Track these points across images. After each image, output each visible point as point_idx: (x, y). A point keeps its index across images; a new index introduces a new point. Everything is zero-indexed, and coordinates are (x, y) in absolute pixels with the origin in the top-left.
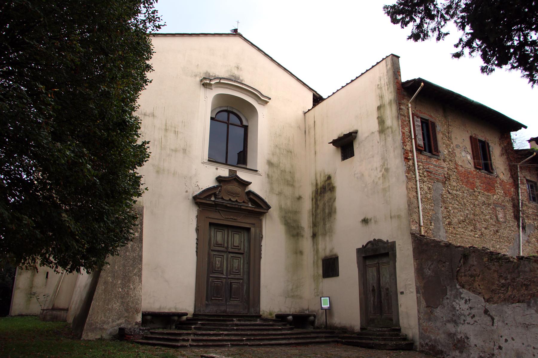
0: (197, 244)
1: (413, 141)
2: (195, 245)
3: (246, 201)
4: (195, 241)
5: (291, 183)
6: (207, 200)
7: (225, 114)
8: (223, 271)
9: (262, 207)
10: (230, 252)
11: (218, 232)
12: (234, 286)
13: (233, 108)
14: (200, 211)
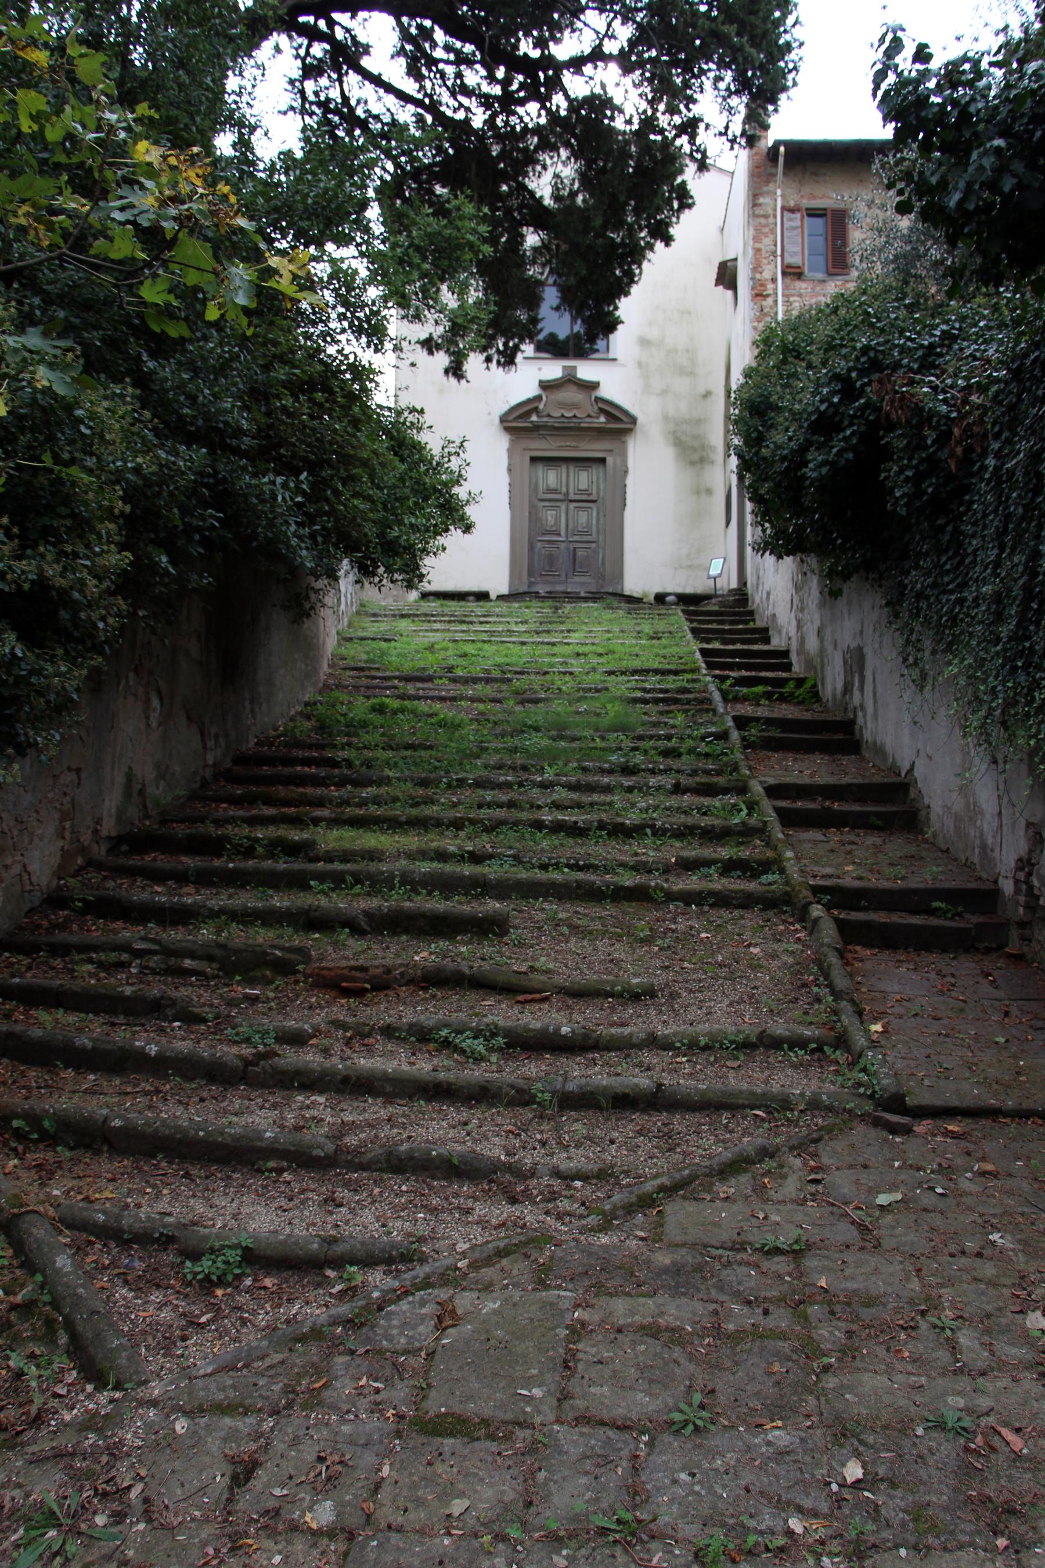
1: (779, 259)
2: (507, 494)
5: (688, 371)
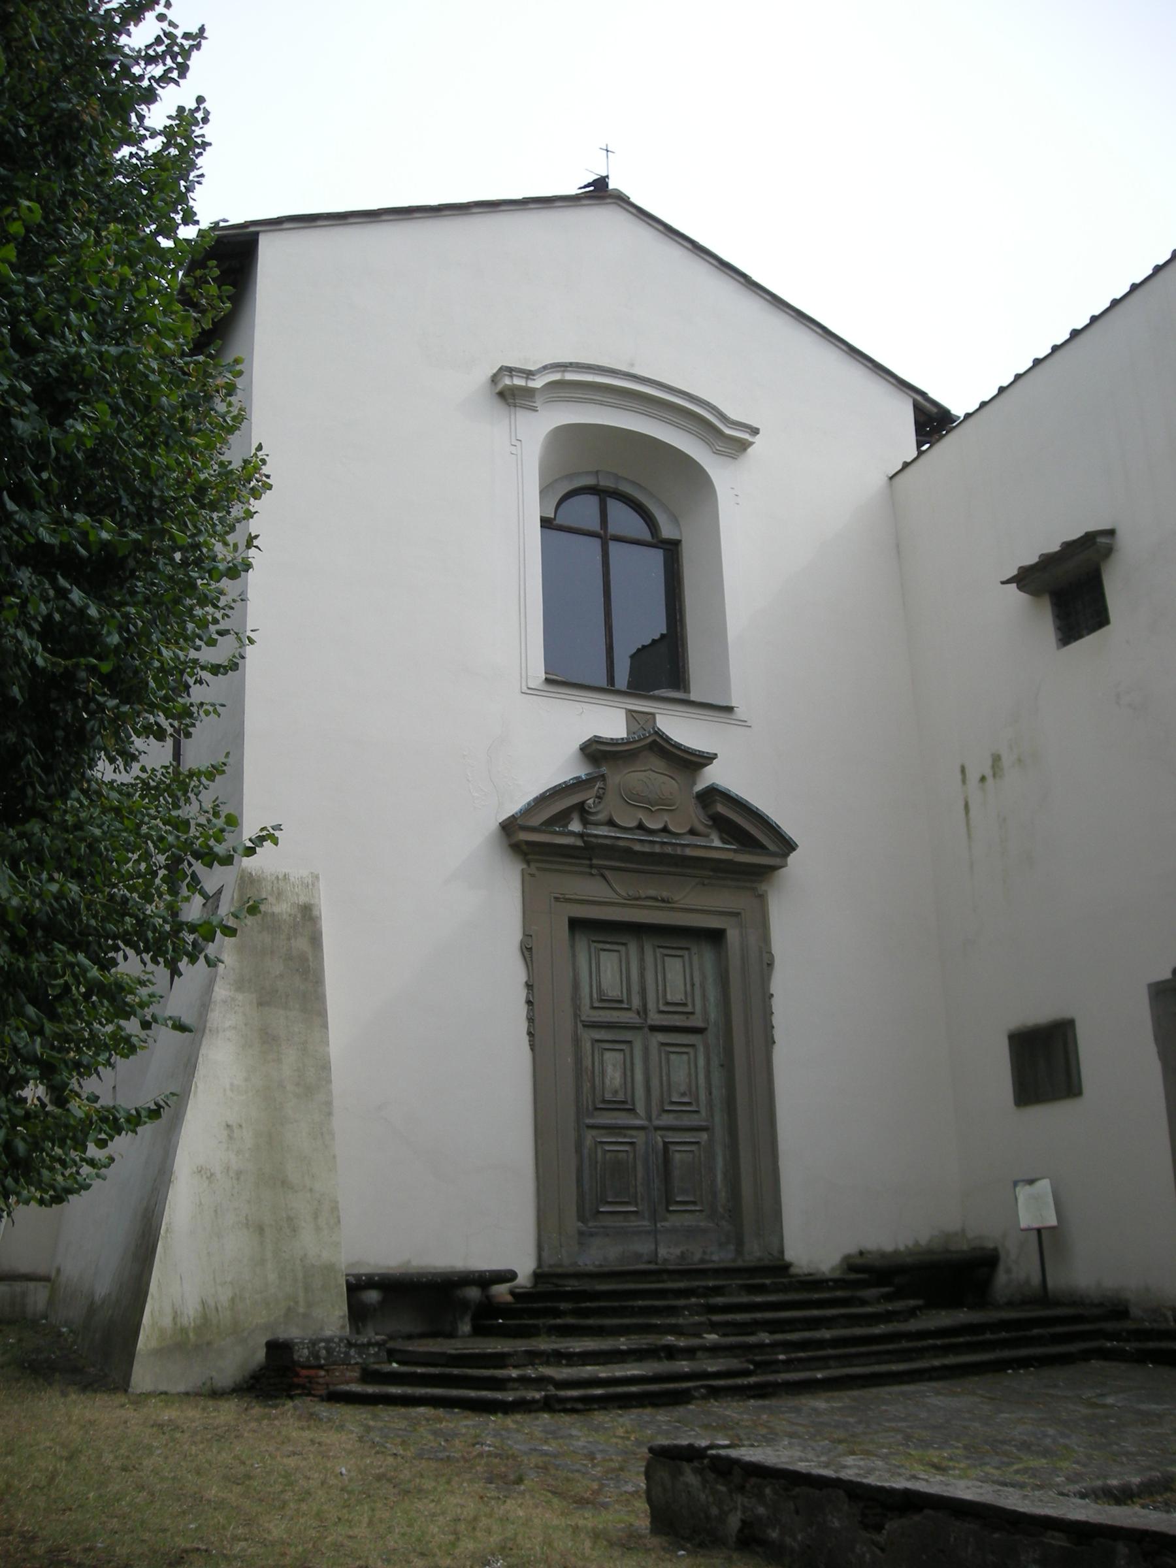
0: (529, 1003)
2: (522, 1010)
3: (700, 828)
4: (521, 994)
6: (555, 833)
7: (592, 501)
8: (633, 1104)
9: (763, 847)
10: (654, 1029)
11: (602, 954)
12: (677, 1156)
13: (617, 477)
14: (532, 875)
